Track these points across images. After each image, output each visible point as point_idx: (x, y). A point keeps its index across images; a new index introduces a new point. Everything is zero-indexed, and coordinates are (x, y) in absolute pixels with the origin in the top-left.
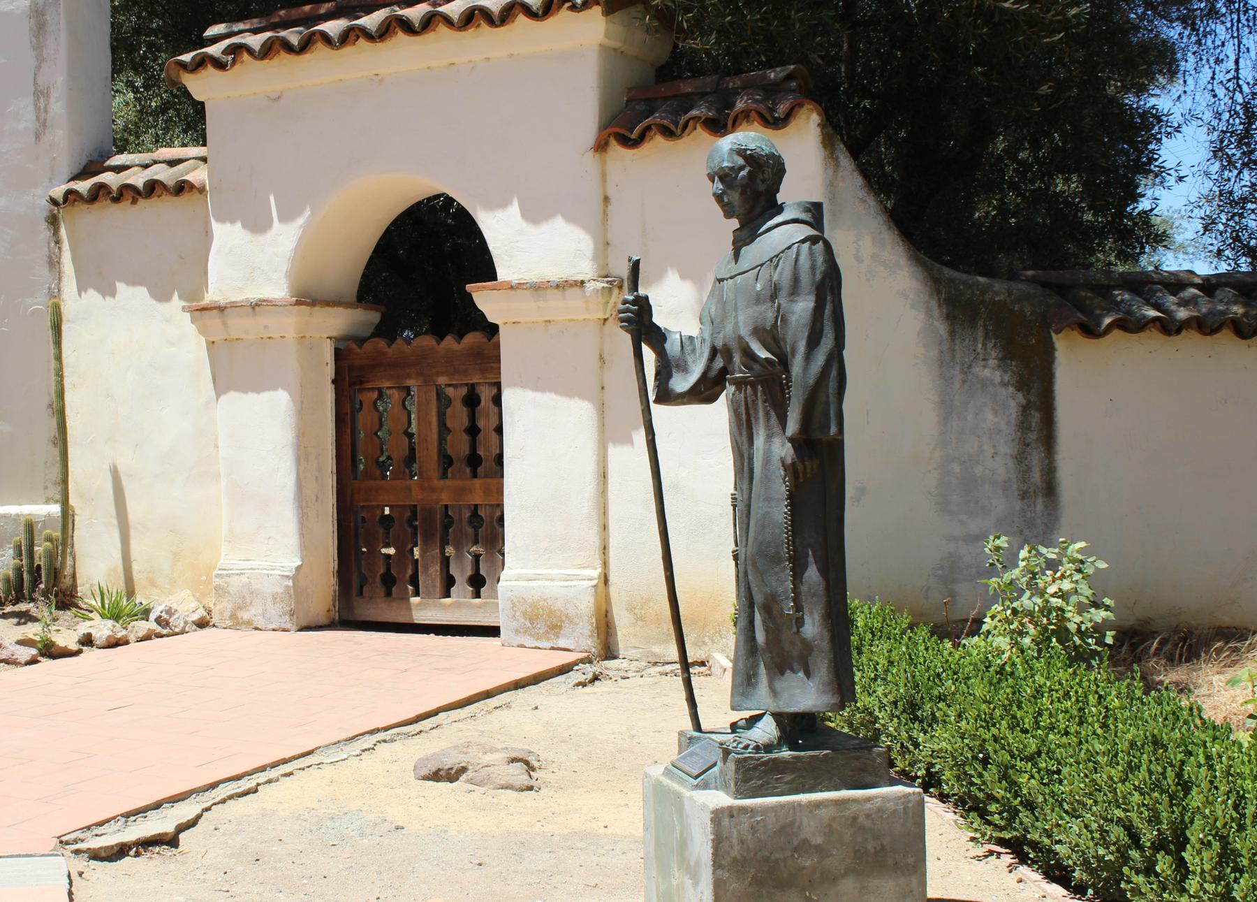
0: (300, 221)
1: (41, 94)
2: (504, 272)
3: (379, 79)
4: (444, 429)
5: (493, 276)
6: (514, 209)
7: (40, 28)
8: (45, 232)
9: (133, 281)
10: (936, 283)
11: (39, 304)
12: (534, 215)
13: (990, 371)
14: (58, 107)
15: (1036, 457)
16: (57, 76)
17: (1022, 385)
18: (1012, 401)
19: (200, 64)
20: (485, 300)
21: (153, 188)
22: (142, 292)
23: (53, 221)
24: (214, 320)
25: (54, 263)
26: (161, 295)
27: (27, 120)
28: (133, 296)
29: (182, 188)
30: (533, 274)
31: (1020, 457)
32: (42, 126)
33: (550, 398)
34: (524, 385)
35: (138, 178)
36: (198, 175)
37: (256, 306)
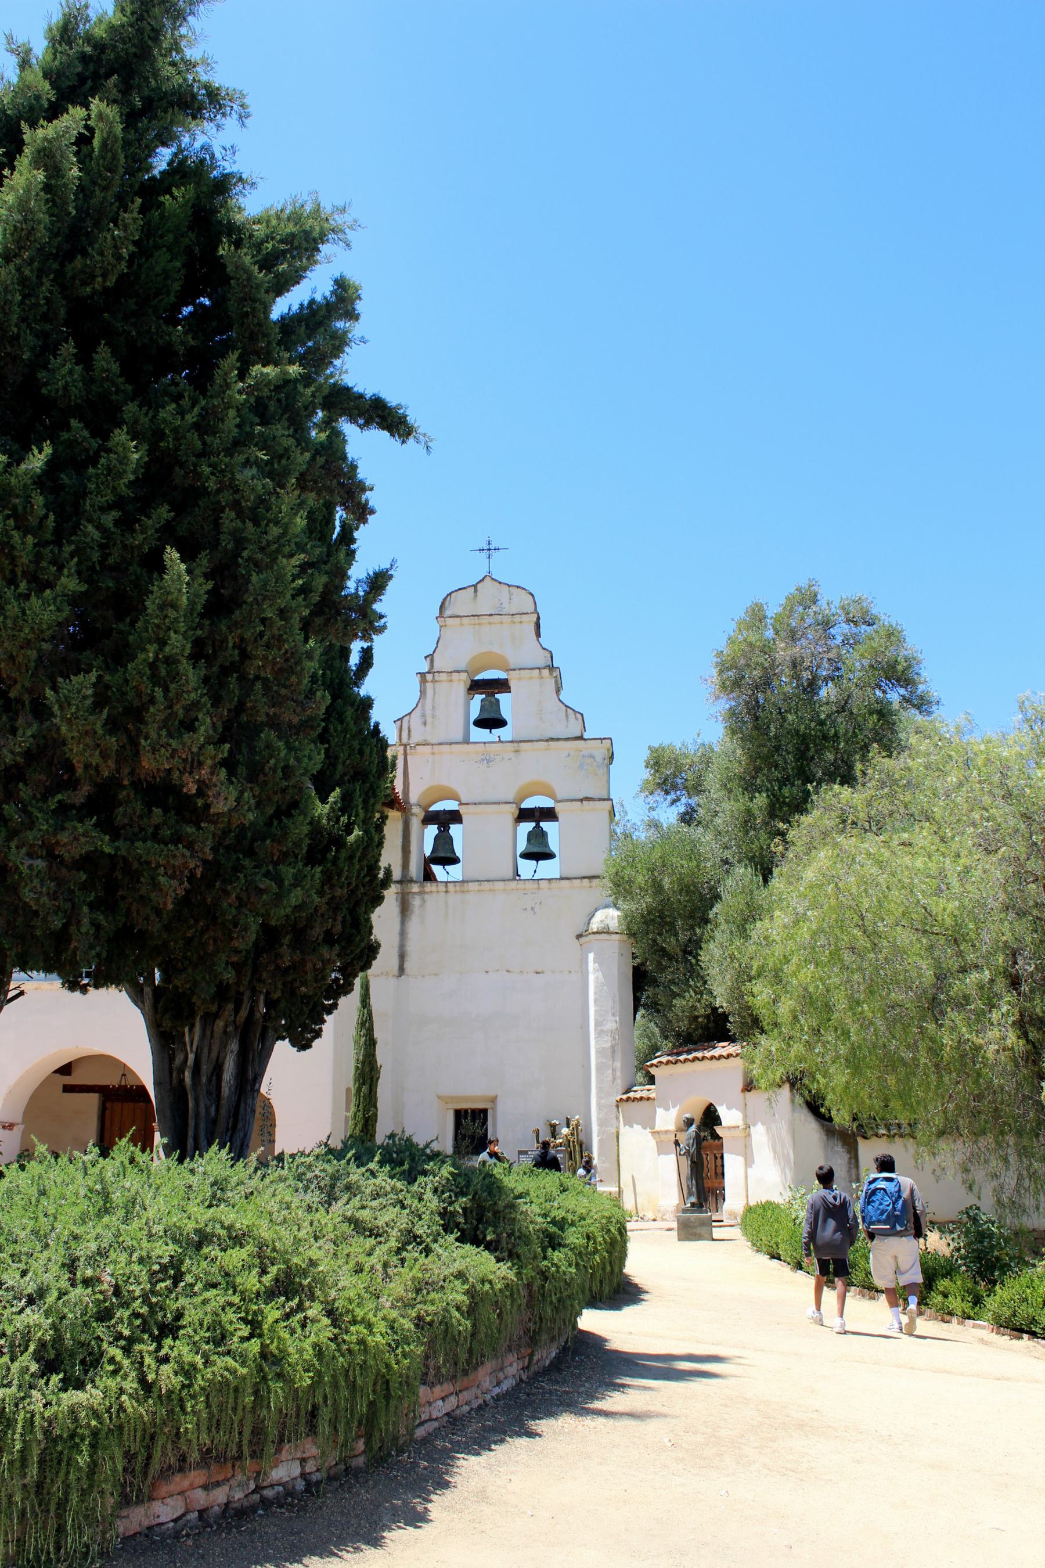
0: (677, 1108)
1: (614, 1070)
2: (725, 1122)
3: (695, 1071)
4: (716, 1167)
5: (721, 1124)
6: (725, 1106)
7: (613, 1052)
8: (615, 1109)
10: (823, 1126)
11: (614, 1130)
12: (729, 1108)
13: (839, 1148)
14: (618, 1074)
15: (854, 1171)
16: (618, 1065)
17: (849, 1152)
18: (846, 1157)
19: (652, 1065)
20: (719, 1130)
21: (641, 1098)
23: (617, 1106)
25: (617, 1118)
26: (645, 1128)
27: (610, 1078)
28: (637, 1128)
29: (648, 1099)
30: (729, 1124)
31: (849, 1171)
32: (614, 1079)
33: (734, 1156)
34: (731, 1153)
35: (638, 1095)
36: (653, 1095)
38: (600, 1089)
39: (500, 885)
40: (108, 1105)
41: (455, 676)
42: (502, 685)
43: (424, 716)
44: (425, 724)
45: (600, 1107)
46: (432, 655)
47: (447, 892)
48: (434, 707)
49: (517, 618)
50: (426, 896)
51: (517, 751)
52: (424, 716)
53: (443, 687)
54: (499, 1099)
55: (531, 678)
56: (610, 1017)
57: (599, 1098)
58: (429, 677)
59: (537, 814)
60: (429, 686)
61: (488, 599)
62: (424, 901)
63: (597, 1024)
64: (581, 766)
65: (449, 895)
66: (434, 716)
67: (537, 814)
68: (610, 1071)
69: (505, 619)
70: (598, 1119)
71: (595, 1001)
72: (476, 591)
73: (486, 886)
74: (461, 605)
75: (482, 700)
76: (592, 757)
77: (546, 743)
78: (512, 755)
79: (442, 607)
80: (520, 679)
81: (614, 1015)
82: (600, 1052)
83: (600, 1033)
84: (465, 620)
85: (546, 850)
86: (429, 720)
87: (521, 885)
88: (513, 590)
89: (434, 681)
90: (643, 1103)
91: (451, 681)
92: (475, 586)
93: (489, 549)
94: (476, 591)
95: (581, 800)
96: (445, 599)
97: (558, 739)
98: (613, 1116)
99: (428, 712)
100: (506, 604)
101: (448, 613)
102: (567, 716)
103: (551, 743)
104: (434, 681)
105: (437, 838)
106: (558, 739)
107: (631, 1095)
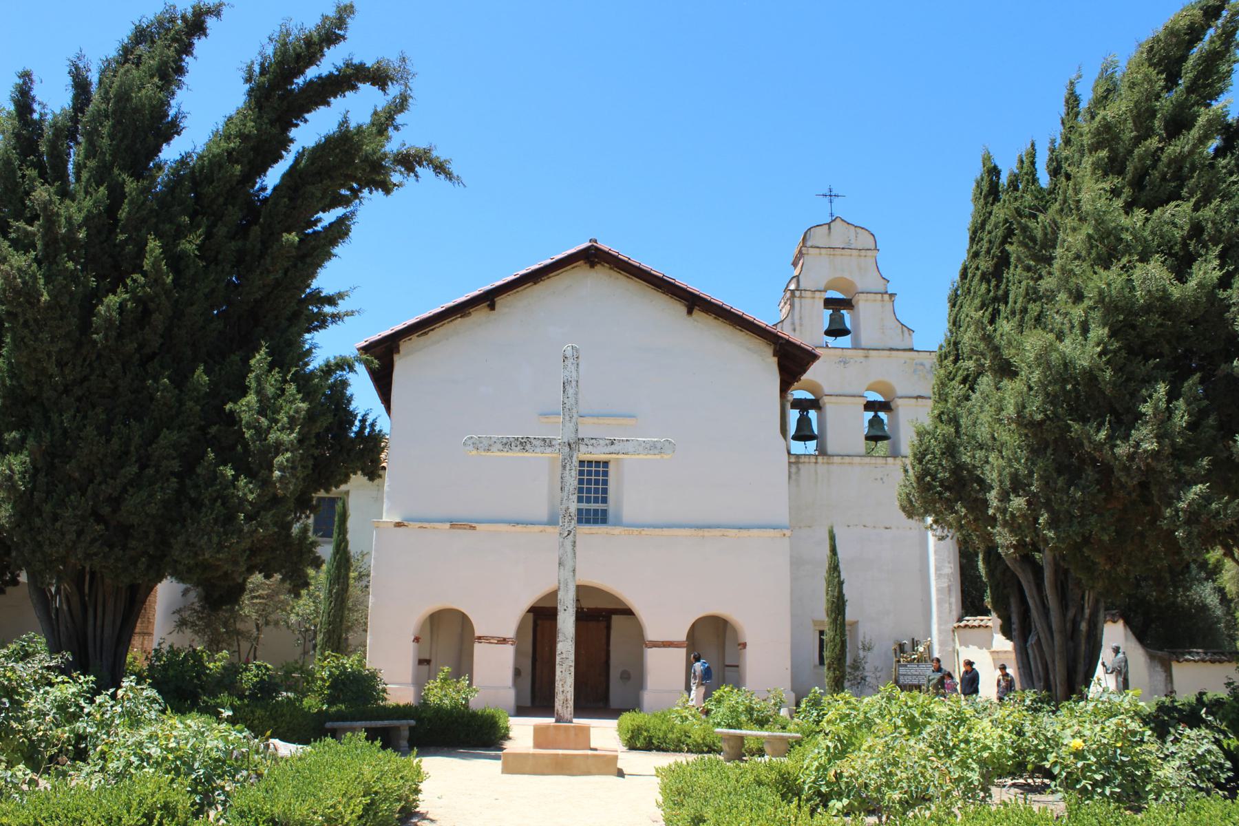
1: (950, 604)
7: (950, 591)
8: (951, 633)
9: (974, 645)
10: (1147, 652)
13: (1159, 669)
14: (954, 607)
15: (1169, 686)
17: (1166, 671)
18: (1164, 675)
21: (980, 626)
22: (976, 647)
23: (953, 631)
24: (996, 656)
25: (954, 640)
26: (981, 648)
27: (947, 610)
31: (1166, 686)
32: (951, 611)
35: (976, 623)
36: (990, 624)
37: (1006, 652)
38: (940, 618)
39: (857, 460)
40: (539, 622)
41: (817, 294)
42: (847, 304)
43: (793, 324)
44: (794, 330)
45: (940, 632)
46: (797, 277)
47: (816, 463)
48: (801, 318)
49: (863, 253)
50: (800, 466)
51: (866, 357)
52: (793, 324)
53: (807, 302)
54: (860, 624)
55: (875, 301)
56: (947, 564)
57: (939, 625)
58: (797, 293)
59: (877, 405)
60: (797, 300)
61: (839, 235)
62: (799, 469)
63: (937, 569)
64: (915, 371)
65: (818, 465)
66: (801, 325)
67: (877, 405)
68: (947, 605)
69: (855, 253)
70: (939, 640)
71: (936, 552)
72: (830, 228)
73: (847, 460)
74: (819, 238)
75: (831, 315)
76: (922, 364)
77: (888, 352)
78: (862, 359)
79: (804, 239)
80: (867, 300)
81: (949, 562)
82: (939, 590)
83: (939, 576)
84: (823, 251)
85: (880, 433)
86: (798, 328)
87: (873, 460)
88: (859, 230)
89: (801, 297)
90: (981, 630)
91: (813, 298)
92: (829, 224)
93: (831, 196)
94: (830, 228)
95: (918, 397)
96: (806, 233)
97: (898, 350)
98: (950, 638)
99: (797, 322)
100: (853, 241)
101: (809, 243)
102: (903, 332)
103: (893, 352)
104: (801, 297)
105: (799, 421)
106: (898, 350)
107: (962, 624)
